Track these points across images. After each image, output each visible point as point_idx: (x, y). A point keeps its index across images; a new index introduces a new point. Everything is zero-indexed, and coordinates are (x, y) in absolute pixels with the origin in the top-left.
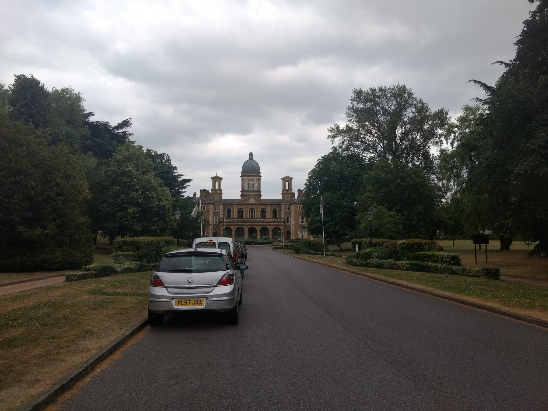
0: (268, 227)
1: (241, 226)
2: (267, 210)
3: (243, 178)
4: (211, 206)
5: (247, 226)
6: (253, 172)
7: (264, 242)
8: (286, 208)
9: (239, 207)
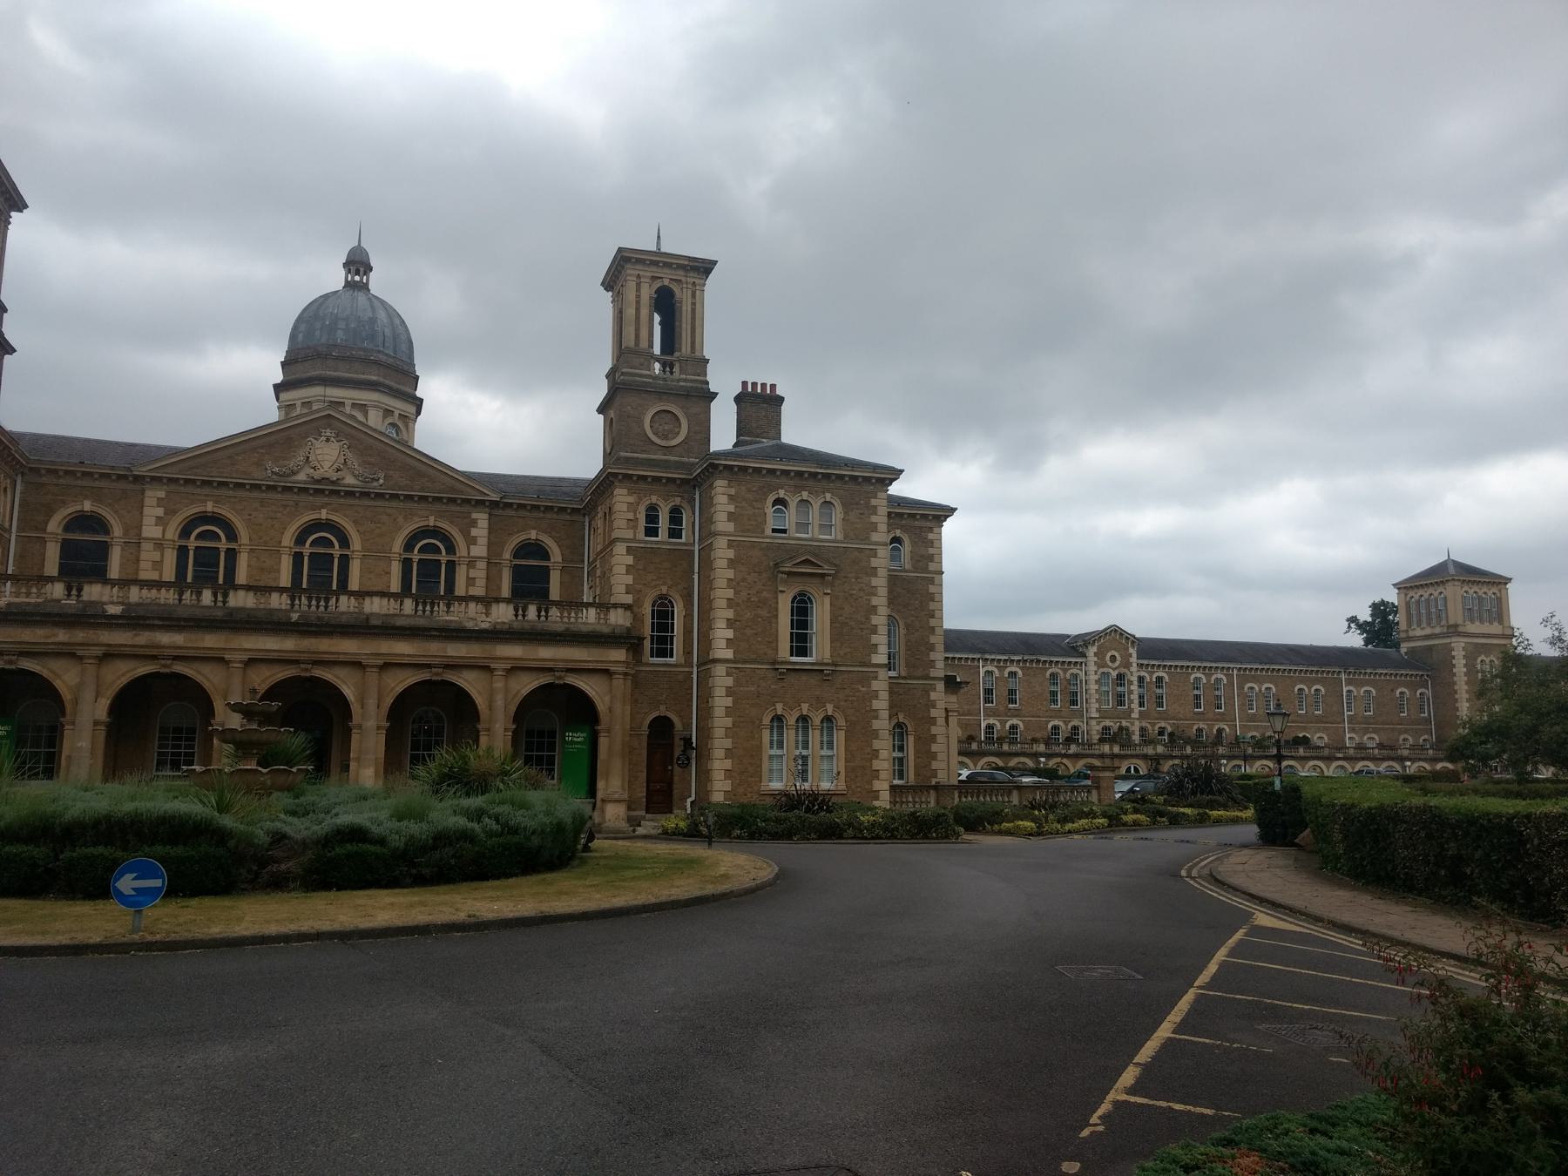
0: (469, 682)
1: (179, 668)
2: (462, 550)
5: (250, 662)
6: (367, 362)
7: (443, 838)
8: (652, 517)
9: (195, 509)
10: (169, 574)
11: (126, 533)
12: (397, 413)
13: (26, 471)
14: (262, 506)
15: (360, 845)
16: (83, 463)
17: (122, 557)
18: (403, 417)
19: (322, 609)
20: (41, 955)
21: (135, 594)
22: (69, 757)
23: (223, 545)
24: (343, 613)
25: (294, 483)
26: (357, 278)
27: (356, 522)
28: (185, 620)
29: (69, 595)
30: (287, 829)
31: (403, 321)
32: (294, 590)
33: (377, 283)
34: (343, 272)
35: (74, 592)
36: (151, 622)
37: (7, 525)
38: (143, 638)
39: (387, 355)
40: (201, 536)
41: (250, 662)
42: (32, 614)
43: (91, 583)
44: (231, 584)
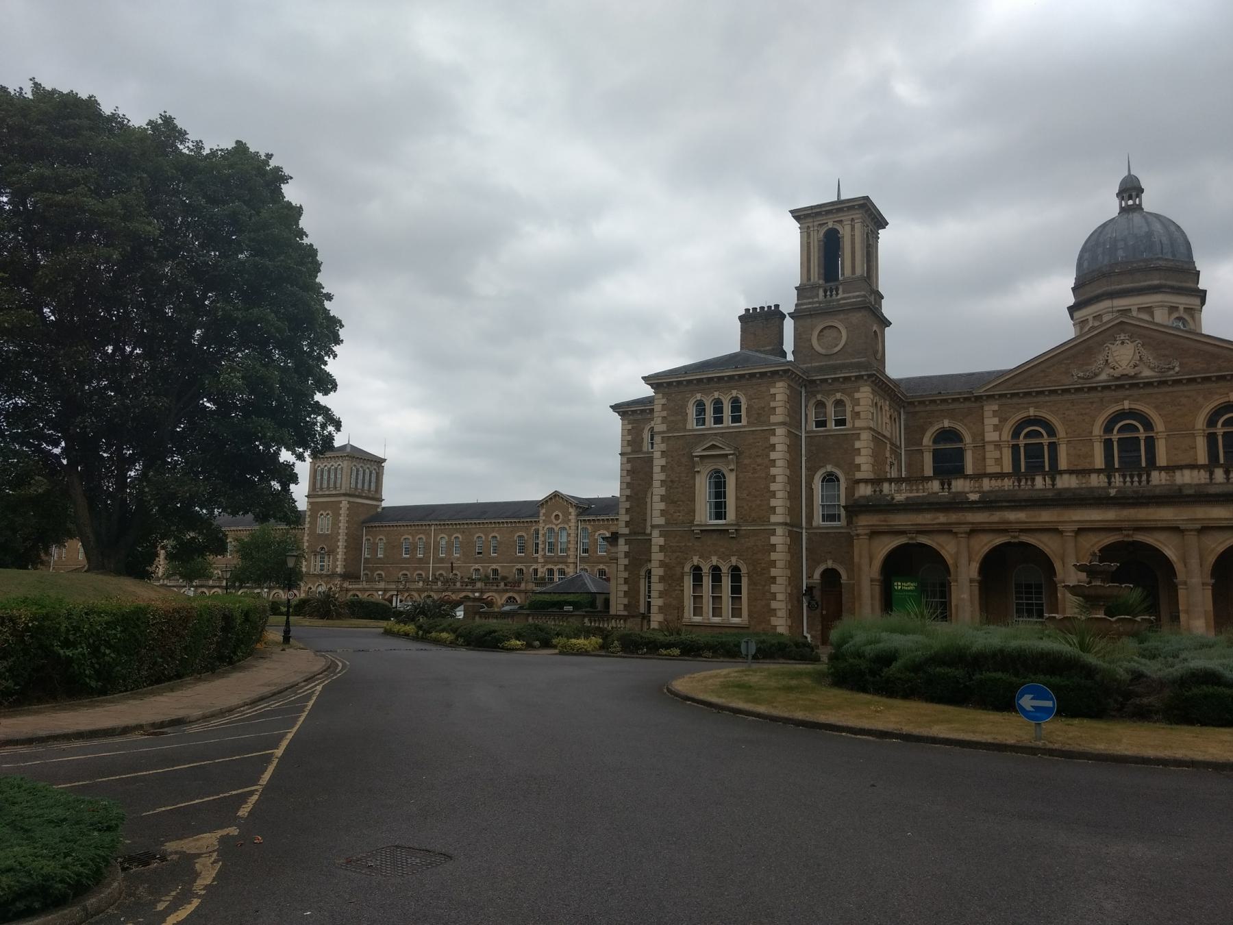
4: (780, 390)
5: (1080, 531)
6: (1148, 270)
10: (1008, 467)
11: (974, 440)
12: (1181, 307)
13: (906, 405)
14: (1073, 406)
15: (1216, 687)
16: (940, 393)
17: (973, 457)
18: (1189, 310)
19: (1136, 484)
20: (975, 748)
21: (987, 484)
22: (957, 606)
23: (1045, 440)
24: (1156, 486)
25: (1097, 383)
26: (1130, 202)
27: (1157, 408)
28: (1025, 501)
29: (943, 489)
30: (1143, 669)
31: (1179, 227)
32: (1109, 470)
33: (1149, 202)
34: (1117, 201)
35: (946, 486)
36: (1000, 504)
37: (898, 444)
38: (997, 516)
39: (1166, 259)
40: (1027, 435)
41: (1080, 531)
42: (922, 504)
43: (957, 478)
44: (1055, 472)
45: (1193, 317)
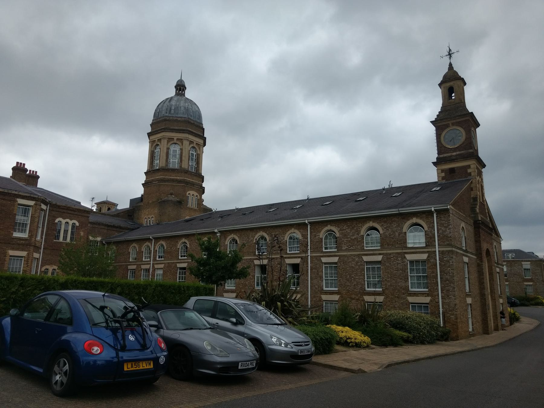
3: (155, 137)
45: (200, 149)
